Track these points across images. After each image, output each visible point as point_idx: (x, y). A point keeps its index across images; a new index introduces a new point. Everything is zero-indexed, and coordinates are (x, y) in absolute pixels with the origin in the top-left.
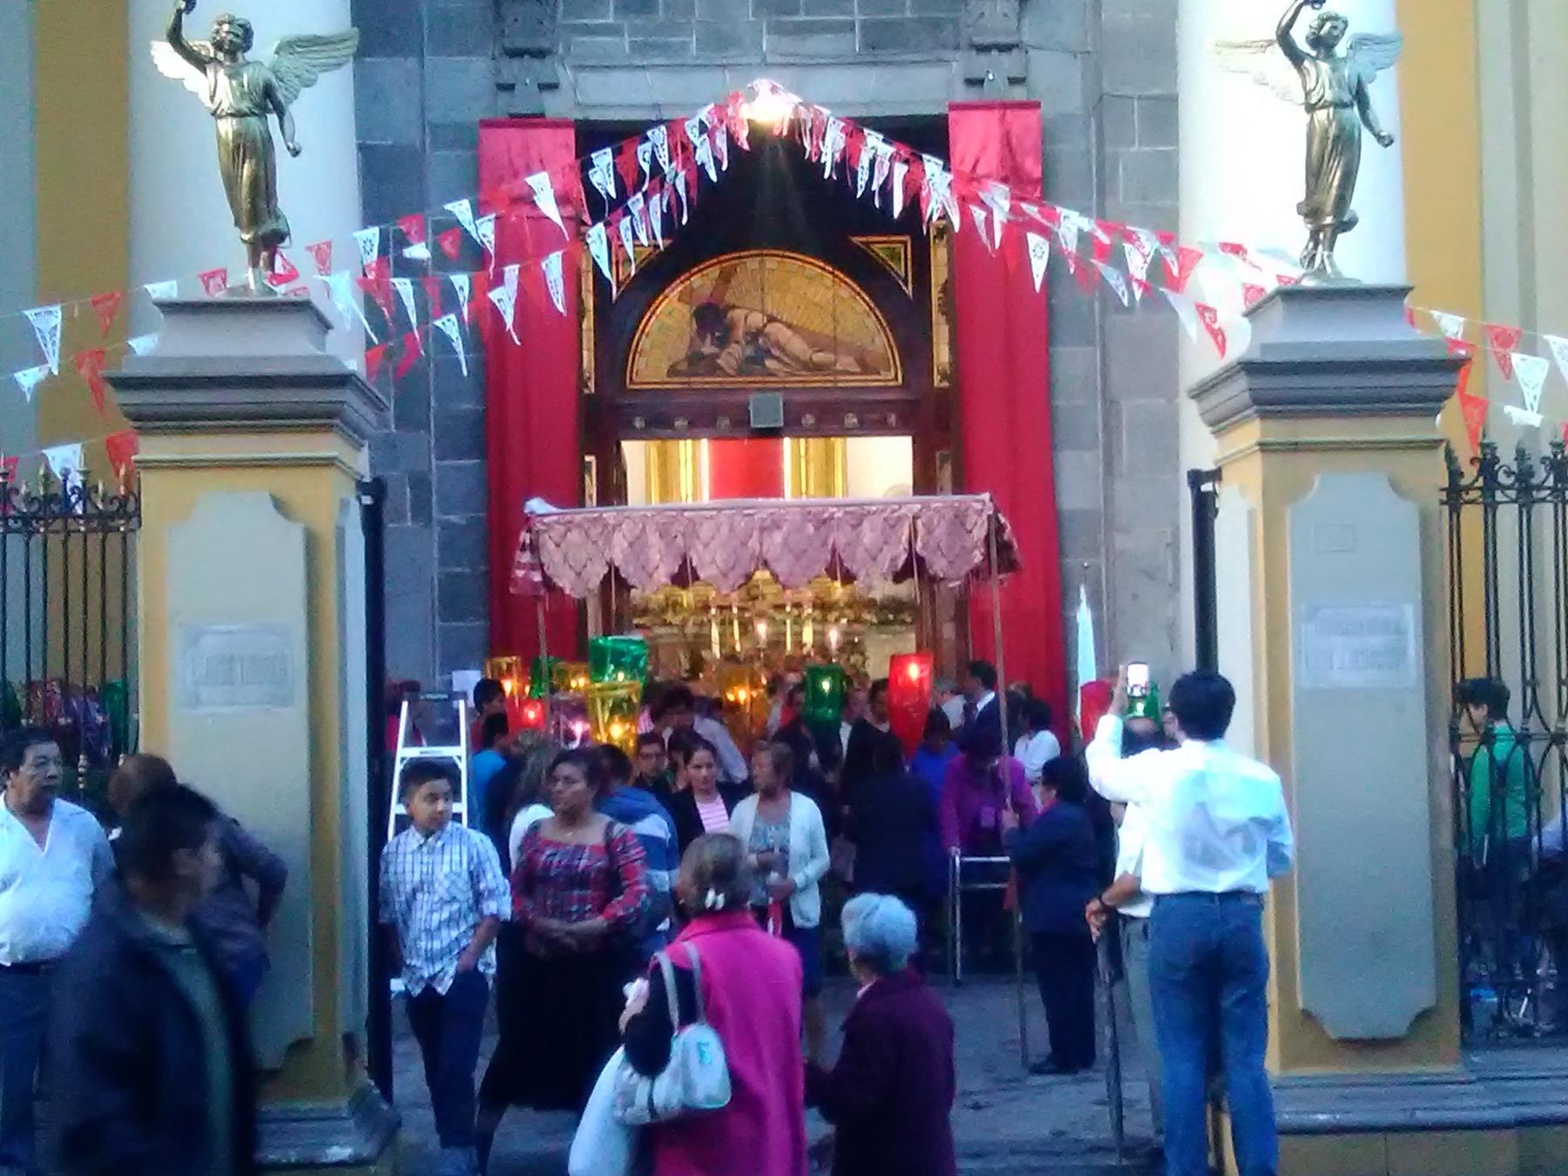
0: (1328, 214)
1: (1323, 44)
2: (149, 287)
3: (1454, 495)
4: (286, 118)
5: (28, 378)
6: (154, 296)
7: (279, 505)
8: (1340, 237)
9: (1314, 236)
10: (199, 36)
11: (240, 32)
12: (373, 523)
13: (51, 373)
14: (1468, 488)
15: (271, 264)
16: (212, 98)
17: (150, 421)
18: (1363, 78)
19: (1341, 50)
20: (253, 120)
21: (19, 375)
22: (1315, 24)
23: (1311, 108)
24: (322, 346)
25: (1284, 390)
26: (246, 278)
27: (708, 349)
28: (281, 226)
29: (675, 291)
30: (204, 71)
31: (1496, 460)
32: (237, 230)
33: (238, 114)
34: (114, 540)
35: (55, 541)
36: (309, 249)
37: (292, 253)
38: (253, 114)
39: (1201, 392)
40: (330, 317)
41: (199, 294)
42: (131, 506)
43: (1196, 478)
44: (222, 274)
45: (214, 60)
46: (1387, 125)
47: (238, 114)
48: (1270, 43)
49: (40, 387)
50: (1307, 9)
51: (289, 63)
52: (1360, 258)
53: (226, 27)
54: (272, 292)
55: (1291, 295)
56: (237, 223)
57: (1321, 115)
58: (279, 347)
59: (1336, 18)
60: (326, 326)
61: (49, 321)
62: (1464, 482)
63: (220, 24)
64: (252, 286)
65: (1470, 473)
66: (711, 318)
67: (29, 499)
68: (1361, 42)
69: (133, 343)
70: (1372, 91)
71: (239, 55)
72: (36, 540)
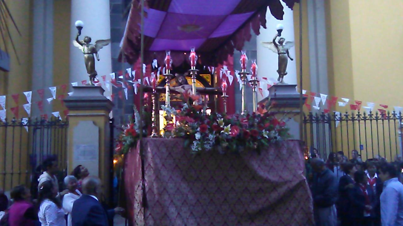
1: (281, 43)
2: (72, 83)
4: (97, 54)
5: (49, 100)
6: (73, 86)
7: (94, 123)
10: (81, 39)
13: (54, 99)
16: (84, 50)
17: (71, 108)
19: (284, 44)
20: (91, 55)
21: (48, 99)
22: (279, 39)
23: (279, 54)
24: (103, 94)
32: (88, 74)
34: (64, 130)
36: (102, 77)
41: (81, 85)
45: (84, 44)
46: (292, 58)
48: (271, 43)
49: (52, 101)
50: (278, 37)
54: (94, 85)
56: (88, 73)
58: (96, 94)
61: (54, 90)
68: (288, 43)
69: (69, 93)
70: (289, 51)
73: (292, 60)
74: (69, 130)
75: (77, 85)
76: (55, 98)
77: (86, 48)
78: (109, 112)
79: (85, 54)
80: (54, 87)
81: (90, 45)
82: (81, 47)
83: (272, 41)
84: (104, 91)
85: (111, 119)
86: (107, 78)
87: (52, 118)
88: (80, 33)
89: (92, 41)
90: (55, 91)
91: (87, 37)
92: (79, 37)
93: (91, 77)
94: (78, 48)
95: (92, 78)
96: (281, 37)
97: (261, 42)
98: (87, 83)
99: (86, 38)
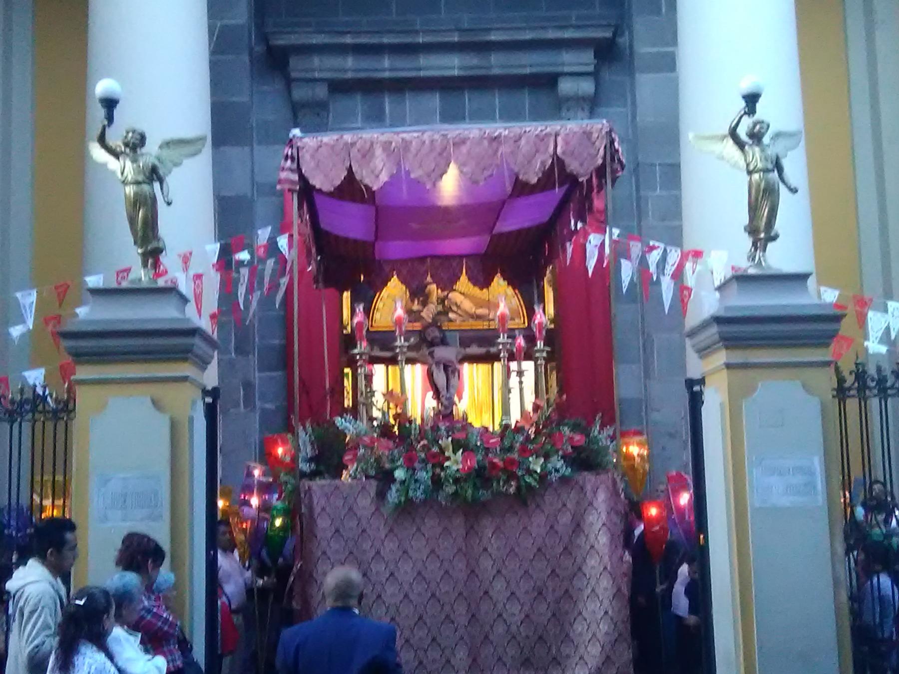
0: (761, 231)
1: (756, 136)
3: (841, 392)
4: (165, 185)
7: (155, 403)
8: (770, 246)
9: (755, 244)
10: (115, 139)
11: (138, 137)
12: (211, 413)
14: (849, 389)
16: (122, 173)
17: (81, 357)
18: (780, 156)
19: (766, 140)
20: (146, 188)
22: (751, 125)
23: (750, 173)
24: (183, 312)
25: (742, 333)
26: (141, 275)
28: (161, 245)
30: (118, 158)
31: (864, 372)
32: (135, 247)
33: (137, 183)
35: (26, 427)
37: (169, 260)
38: (144, 182)
39: (692, 334)
41: (114, 285)
42: (71, 406)
43: (690, 383)
44: (128, 270)
45: (122, 153)
46: (793, 182)
47: (137, 183)
50: (745, 118)
51: (165, 153)
52: (782, 256)
53: (130, 135)
55: (741, 279)
56: (135, 243)
57: (756, 176)
58: (162, 313)
59: (763, 122)
62: (847, 385)
63: (128, 133)
65: (850, 380)
67: (13, 402)
68: (778, 135)
70: (786, 163)
71: (138, 150)
72: (16, 426)
73: (794, 191)
74: (77, 425)
76: (31, 327)
77: (129, 164)
78: (203, 369)
79: (125, 183)
81: (142, 155)
82: (113, 164)
83: (726, 131)
85: (208, 391)
86: (193, 261)
87: (22, 391)
88: (110, 118)
89: (148, 141)
92: (108, 132)
93: (145, 256)
94: (104, 165)
95: (150, 261)
96: (758, 116)
97: (691, 136)
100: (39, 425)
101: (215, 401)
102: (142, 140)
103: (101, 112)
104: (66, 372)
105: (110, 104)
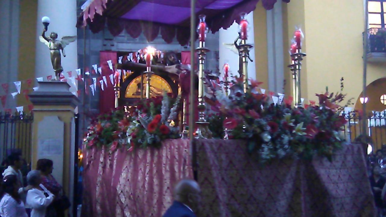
2: (37, 78)
4: (63, 50)
5: (14, 94)
6: (39, 81)
7: (60, 118)
11: (55, 35)
12: (77, 121)
13: (18, 93)
15: (60, 76)
17: (35, 103)
20: (57, 51)
24: (69, 90)
26: (55, 77)
27: (139, 91)
28: (61, 69)
29: (134, 81)
30: (48, 41)
32: (53, 69)
35: (17, 124)
36: (67, 72)
40: (70, 85)
41: (47, 81)
42: (32, 118)
44: (51, 76)
49: (16, 95)
56: (54, 68)
58: (61, 90)
60: (69, 86)
61: (18, 84)
63: (52, 33)
64: (56, 79)
66: (140, 86)
69: (34, 88)
72: (14, 124)
74: (33, 124)
75: (42, 81)
76: (19, 93)
77: (52, 44)
78: (75, 108)
79: (51, 49)
80: (19, 82)
81: (57, 41)
82: (47, 43)
84: (70, 87)
88: (46, 29)
89: (58, 37)
90: (19, 86)
91: (54, 33)
92: (45, 33)
93: (56, 73)
95: (58, 74)
98: (53, 78)
99: (53, 34)
100: (21, 125)
101: (78, 118)
102: (56, 36)
103: (44, 27)
104: (30, 108)
105: (46, 24)
